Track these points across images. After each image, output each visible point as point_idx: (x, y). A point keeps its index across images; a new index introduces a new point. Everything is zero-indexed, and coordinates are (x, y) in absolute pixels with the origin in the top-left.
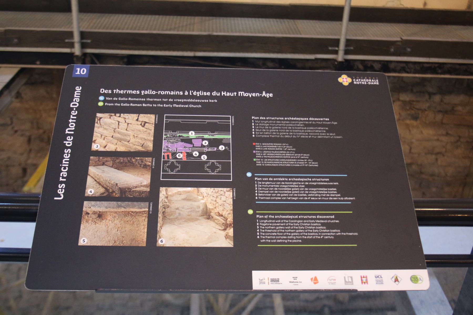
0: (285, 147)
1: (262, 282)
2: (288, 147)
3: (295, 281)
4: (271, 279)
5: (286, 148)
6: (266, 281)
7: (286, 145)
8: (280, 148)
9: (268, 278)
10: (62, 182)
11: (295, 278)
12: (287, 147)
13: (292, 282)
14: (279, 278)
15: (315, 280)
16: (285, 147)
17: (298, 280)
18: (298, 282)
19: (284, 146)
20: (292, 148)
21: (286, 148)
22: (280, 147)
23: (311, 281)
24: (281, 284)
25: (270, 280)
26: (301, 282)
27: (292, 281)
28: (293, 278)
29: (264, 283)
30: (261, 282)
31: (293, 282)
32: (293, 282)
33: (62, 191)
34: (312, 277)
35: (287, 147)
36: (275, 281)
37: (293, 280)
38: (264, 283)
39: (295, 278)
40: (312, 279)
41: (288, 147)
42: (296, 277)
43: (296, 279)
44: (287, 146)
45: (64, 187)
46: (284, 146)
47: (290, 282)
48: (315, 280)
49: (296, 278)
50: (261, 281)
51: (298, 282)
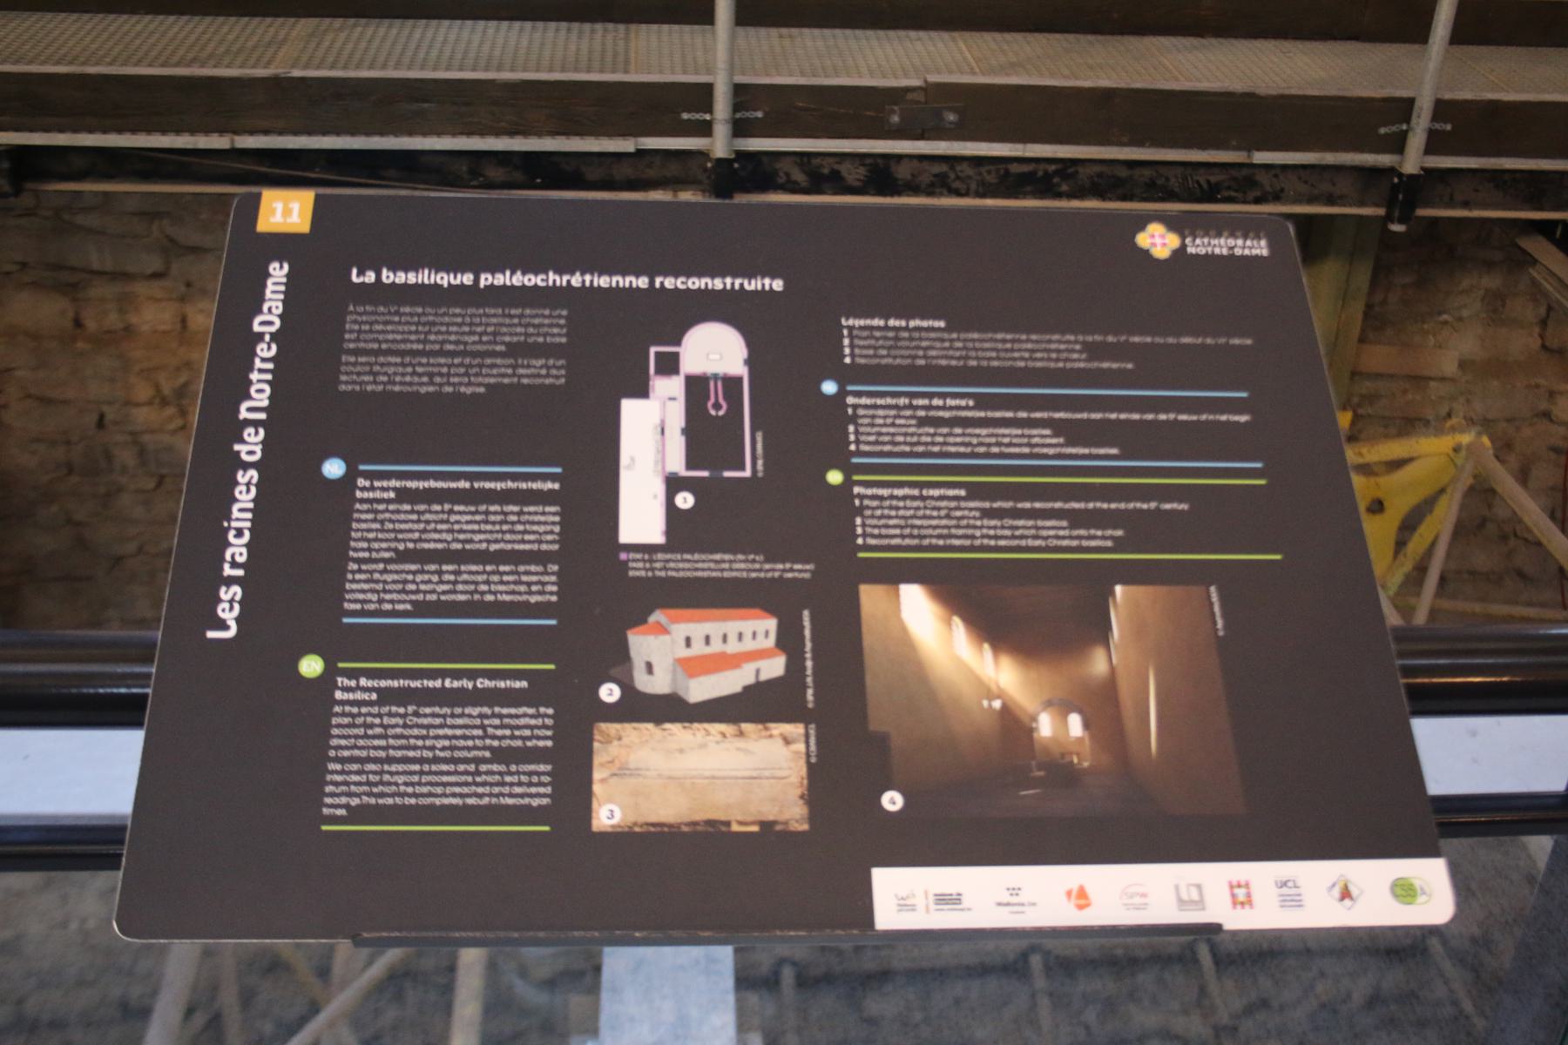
1: (905, 905)
3: (1014, 900)
4: (936, 895)
6: (920, 901)
11: (1015, 891)
14: (960, 892)
15: (1081, 897)
18: (1023, 905)
23: (1064, 898)
25: (931, 899)
26: (1034, 904)
27: (1005, 901)
28: (1008, 889)
29: (912, 908)
30: (905, 906)
31: (1008, 904)
32: (1008, 904)
36: (947, 900)
37: (1006, 898)
38: (912, 908)
39: (1014, 889)
40: (1069, 894)
43: (1017, 895)
47: (999, 904)
50: (902, 902)
51: (1023, 905)
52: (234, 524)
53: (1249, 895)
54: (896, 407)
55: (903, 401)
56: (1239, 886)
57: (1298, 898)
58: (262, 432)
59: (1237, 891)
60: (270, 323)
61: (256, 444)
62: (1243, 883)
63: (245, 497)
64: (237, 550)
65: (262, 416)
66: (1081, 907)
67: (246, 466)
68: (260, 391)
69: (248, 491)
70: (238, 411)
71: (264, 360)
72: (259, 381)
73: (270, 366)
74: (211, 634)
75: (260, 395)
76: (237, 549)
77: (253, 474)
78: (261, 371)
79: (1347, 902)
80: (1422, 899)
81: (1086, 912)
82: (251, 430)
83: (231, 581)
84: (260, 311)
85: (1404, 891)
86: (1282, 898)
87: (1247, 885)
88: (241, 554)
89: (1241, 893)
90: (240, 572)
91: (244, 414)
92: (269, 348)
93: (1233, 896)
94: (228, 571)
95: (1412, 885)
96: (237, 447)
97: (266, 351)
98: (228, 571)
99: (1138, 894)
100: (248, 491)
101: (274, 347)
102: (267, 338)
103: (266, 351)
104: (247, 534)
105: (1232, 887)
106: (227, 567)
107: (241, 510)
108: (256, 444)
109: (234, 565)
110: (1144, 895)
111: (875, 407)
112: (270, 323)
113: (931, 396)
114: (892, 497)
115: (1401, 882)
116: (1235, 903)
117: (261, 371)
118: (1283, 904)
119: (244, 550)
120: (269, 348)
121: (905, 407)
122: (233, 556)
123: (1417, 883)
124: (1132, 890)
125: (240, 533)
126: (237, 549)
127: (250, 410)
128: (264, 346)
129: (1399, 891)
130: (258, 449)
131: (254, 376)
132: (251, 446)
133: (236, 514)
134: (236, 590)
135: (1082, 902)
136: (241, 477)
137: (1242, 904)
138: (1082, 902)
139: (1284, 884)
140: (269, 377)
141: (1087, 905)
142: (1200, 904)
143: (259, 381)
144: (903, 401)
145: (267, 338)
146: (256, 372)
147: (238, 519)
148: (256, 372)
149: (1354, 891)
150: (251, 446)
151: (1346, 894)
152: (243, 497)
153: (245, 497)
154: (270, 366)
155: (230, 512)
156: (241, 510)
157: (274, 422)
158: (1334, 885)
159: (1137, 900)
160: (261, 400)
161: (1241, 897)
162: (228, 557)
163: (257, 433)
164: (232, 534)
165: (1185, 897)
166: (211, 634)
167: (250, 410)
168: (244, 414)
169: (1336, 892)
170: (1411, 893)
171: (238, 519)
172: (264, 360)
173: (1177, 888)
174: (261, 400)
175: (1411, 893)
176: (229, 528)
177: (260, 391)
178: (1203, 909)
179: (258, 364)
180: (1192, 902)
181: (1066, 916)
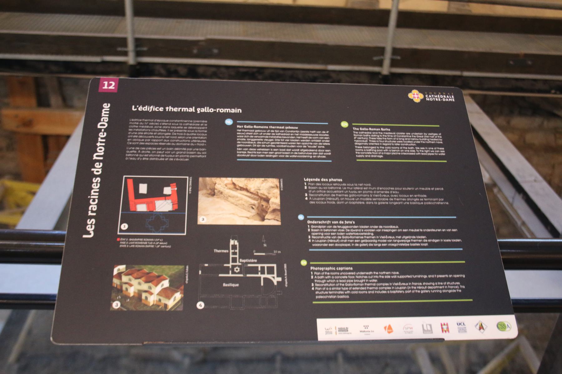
0: (158, 243)
2: (162, 243)
3: (366, 330)
5: (159, 244)
7: (159, 241)
8: (151, 245)
9: (336, 327)
10: (91, 217)
11: (366, 327)
12: (160, 243)
13: (363, 332)
14: (347, 327)
15: (389, 329)
16: (158, 243)
17: (369, 329)
19: (157, 241)
20: (167, 245)
21: (159, 244)
22: (151, 243)
23: (384, 330)
24: (351, 333)
27: (363, 331)
33: (91, 227)
34: (385, 326)
35: (160, 243)
37: (363, 329)
39: (366, 326)
40: (385, 328)
41: (162, 243)
42: (367, 325)
43: (367, 328)
44: (161, 242)
45: (94, 223)
46: (157, 241)
47: (361, 331)
48: (389, 329)
49: (367, 327)
52: (92, 197)
53: (448, 328)
54: (326, 225)
55: (328, 222)
56: (444, 325)
57: (465, 329)
58: (101, 164)
59: (443, 326)
60: (104, 125)
61: (100, 168)
62: (446, 324)
63: (96, 187)
64: (93, 206)
65: (101, 158)
66: (389, 332)
67: (96, 176)
68: (101, 149)
69: (97, 185)
70: (93, 157)
71: (102, 138)
72: (100, 146)
73: (104, 140)
74: (84, 236)
75: (101, 151)
76: (93, 206)
77: (99, 179)
78: (101, 142)
79: (482, 330)
80: (507, 329)
81: (392, 334)
82: (98, 163)
83: (91, 217)
84: (100, 121)
85: (501, 326)
86: (459, 329)
87: (447, 324)
88: (95, 208)
89: (445, 327)
90: (94, 214)
91: (95, 158)
92: (104, 134)
93: (442, 328)
94: (90, 214)
95: (504, 324)
96: (93, 170)
97: (102, 135)
98: (90, 214)
99: (409, 328)
100: (97, 185)
101: (105, 134)
102: (103, 130)
103: (102, 135)
104: (97, 201)
105: (442, 325)
106: (90, 212)
107: (94, 192)
108: (100, 168)
109: (92, 212)
110: (411, 328)
111: (318, 224)
112: (104, 125)
113: (338, 220)
114: (325, 271)
115: (500, 323)
116: (443, 331)
117: (101, 142)
118: (460, 331)
119: (96, 206)
120: (104, 134)
121: (329, 225)
122: (92, 208)
123: (506, 324)
124: (406, 327)
125: (94, 200)
126: (93, 206)
127: (97, 156)
128: (102, 133)
129: (499, 326)
130: (100, 170)
131: (98, 144)
132: (98, 169)
133: (92, 193)
134: (93, 220)
135: (390, 331)
136: (94, 180)
137: (446, 331)
138: (390, 331)
139: (460, 324)
140: (104, 144)
141: (392, 332)
142: (431, 331)
143: (100, 146)
144: (328, 222)
145: (103, 130)
146: (99, 143)
147: (93, 195)
148: (99, 143)
149: (484, 327)
150: (98, 169)
151: (481, 327)
152: (95, 187)
153: (96, 187)
154: (104, 140)
155: (91, 193)
156: (94, 192)
157: (106, 160)
158: (477, 324)
159: (409, 330)
160: (101, 153)
161: (445, 328)
162: (90, 209)
163: (100, 165)
164: (91, 200)
165: (425, 328)
166: (84, 236)
167: (97, 156)
168: (95, 158)
169: (478, 327)
170: (505, 327)
171: (93, 195)
172: (102, 138)
173: (423, 326)
174: (101, 153)
175: (505, 327)
176: (90, 199)
177: (101, 149)
178: (432, 333)
179: (100, 140)
180: (428, 330)
181: (385, 336)
